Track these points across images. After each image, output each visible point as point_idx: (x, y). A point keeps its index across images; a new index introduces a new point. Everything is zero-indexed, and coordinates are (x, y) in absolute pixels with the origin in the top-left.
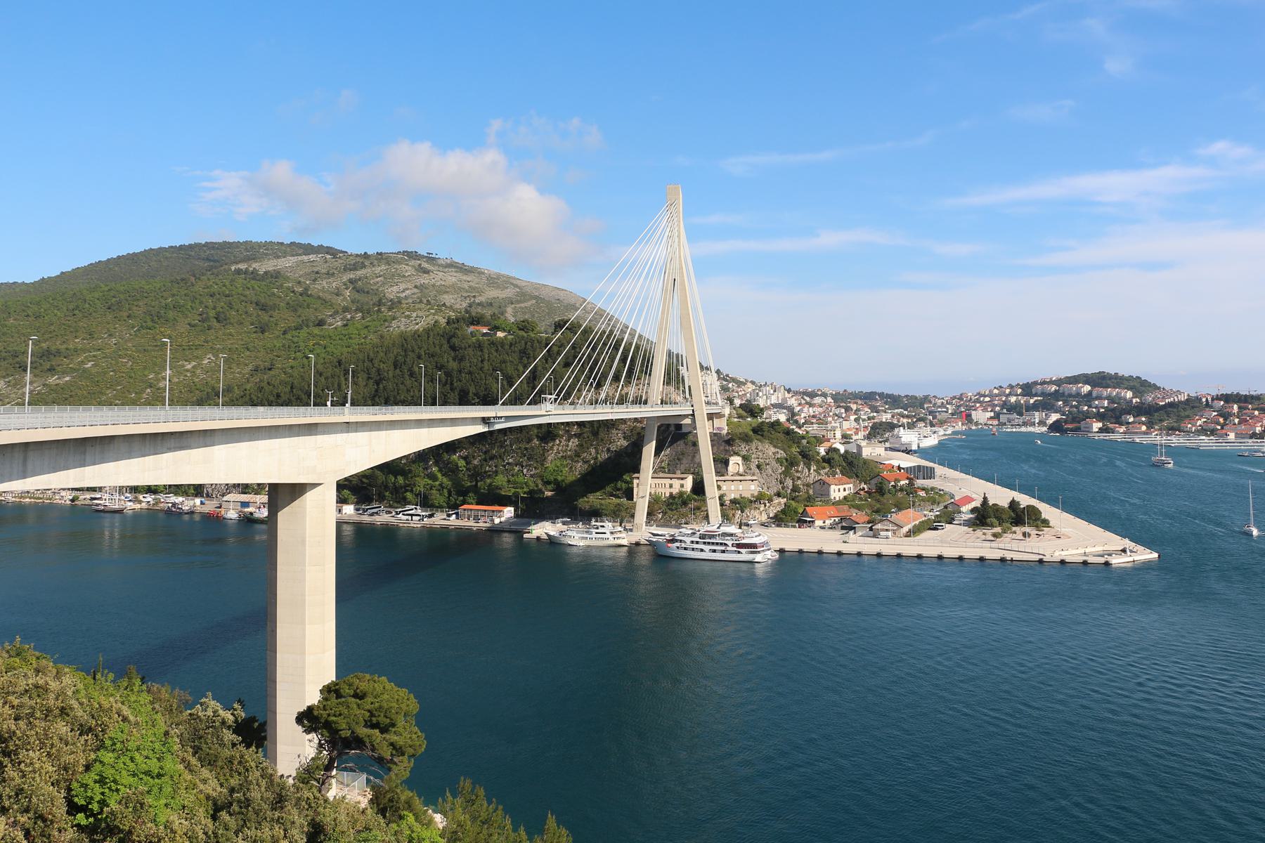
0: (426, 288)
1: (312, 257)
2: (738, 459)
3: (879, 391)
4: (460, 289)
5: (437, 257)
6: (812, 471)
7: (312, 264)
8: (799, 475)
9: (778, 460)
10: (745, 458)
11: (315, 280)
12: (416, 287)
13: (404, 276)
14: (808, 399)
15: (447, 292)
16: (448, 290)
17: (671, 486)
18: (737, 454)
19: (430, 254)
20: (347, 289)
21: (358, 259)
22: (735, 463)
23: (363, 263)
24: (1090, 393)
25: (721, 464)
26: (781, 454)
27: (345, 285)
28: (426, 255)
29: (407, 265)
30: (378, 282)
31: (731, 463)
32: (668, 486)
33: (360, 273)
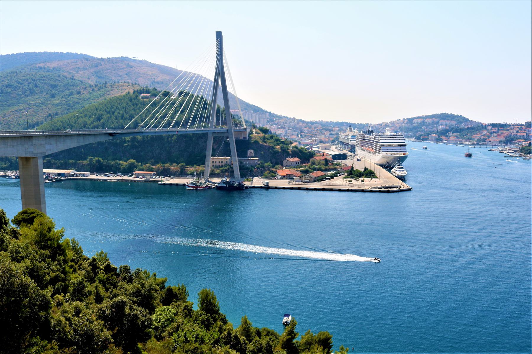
0: (131, 75)
2: (252, 151)
3: (346, 121)
4: (147, 75)
5: (138, 59)
6: (285, 155)
7: (75, 63)
8: (279, 157)
12: (127, 74)
16: (142, 75)
21: (98, 61)
23: (100, 63)
24: (438, 122)
25: (242, 153)
27: (92, 74)
28: (132, 58)
30: (108, 73)
31: (249, 152)
32: (221, 162)
33: (99, 67)
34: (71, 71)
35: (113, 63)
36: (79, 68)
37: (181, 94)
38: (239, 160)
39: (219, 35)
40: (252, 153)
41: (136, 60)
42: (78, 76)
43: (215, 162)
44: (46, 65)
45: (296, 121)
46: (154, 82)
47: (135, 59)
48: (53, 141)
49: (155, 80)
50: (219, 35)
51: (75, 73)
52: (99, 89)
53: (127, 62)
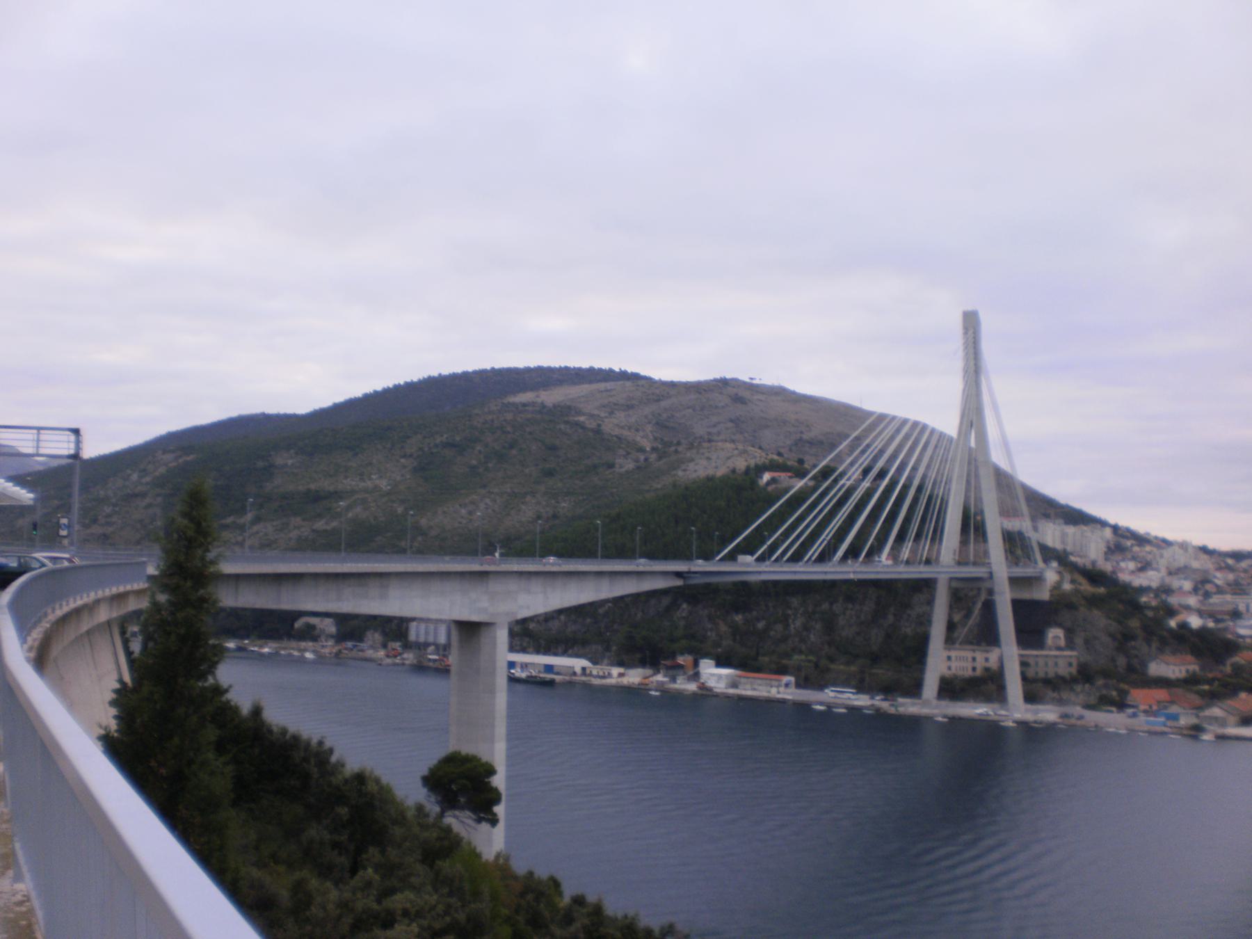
1: (609, 385)
9: (1111, 635)
10: (1069, 632)
11: (611, 413)
12: (731, 421)
13: (716, 407)
14: (1230, 561)
15: (767, 427)
17: (974, 659)
18: (1060, 625)
19: (751, 379)
20: (649, 423)
22: (1055, 635)
23: (668, 393)
25: (1030, 634)
26: (1114, 627)
28: (748, 380)
29: (721, 393)
32: (970, 659)
33: (664, 404)
34: (596, 412)
35: (700, 393)
36: (615, 404)
37: (866, 472)
38: (1021, 656)
39: (971, 322)
40: (1059, 638)
41: (757, 386)
42: (610, 426)
43: (953, 658)
44: (538, 396)
45: (1190, 550)
46: (801, 440)
47: (754, 382)
48: (536, 585)
49: (805, 437)
50: (971, 322)
51: (606, 417)
52: (660, 458)
53: (735, 390)
